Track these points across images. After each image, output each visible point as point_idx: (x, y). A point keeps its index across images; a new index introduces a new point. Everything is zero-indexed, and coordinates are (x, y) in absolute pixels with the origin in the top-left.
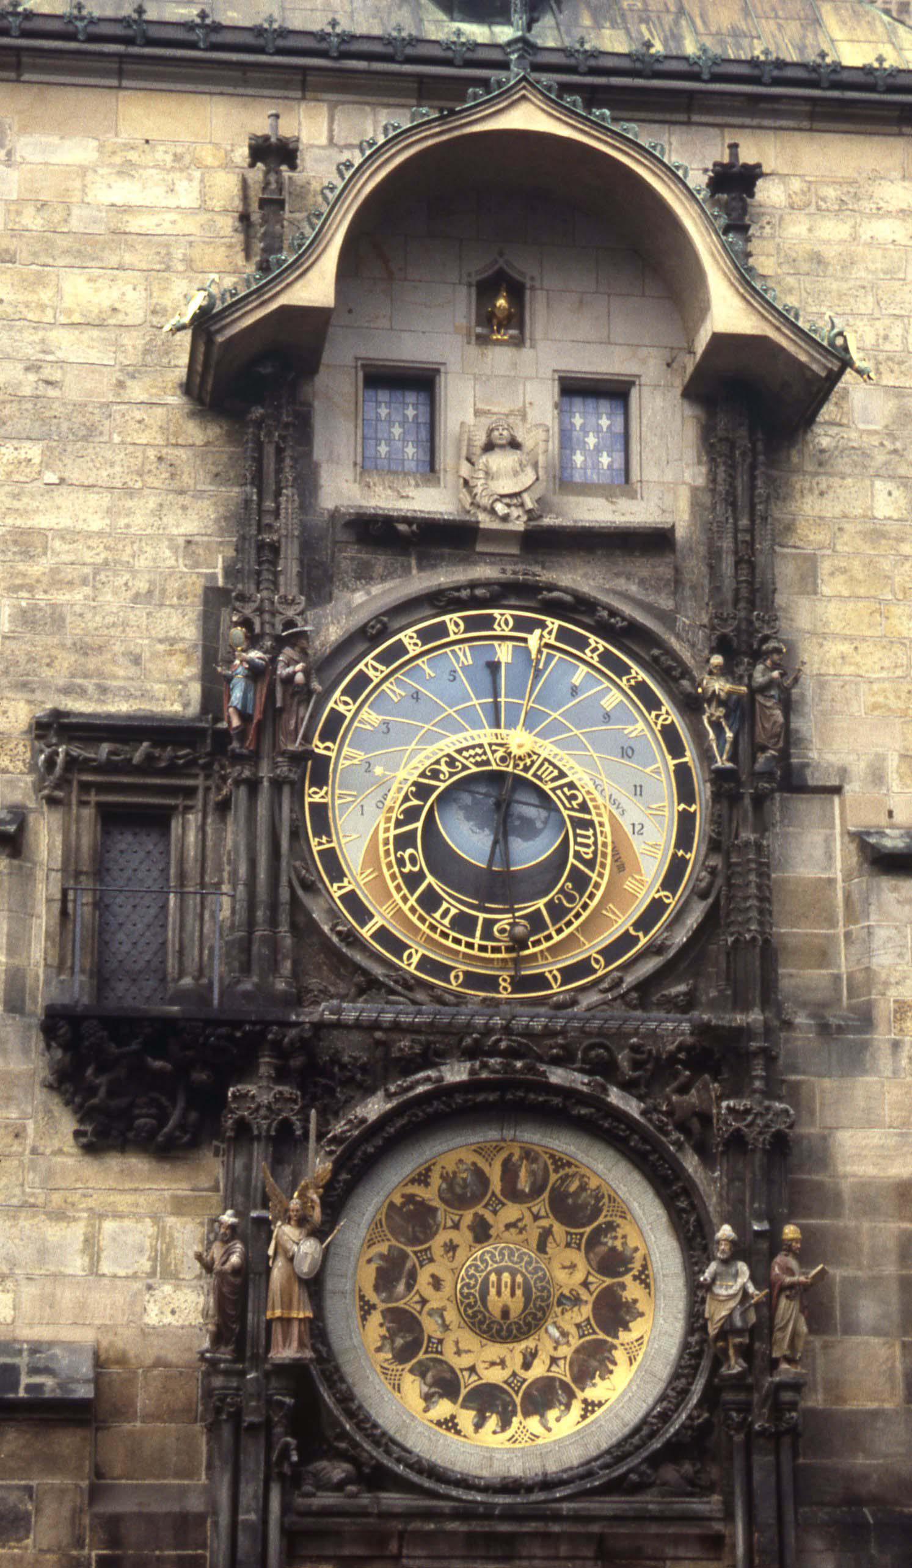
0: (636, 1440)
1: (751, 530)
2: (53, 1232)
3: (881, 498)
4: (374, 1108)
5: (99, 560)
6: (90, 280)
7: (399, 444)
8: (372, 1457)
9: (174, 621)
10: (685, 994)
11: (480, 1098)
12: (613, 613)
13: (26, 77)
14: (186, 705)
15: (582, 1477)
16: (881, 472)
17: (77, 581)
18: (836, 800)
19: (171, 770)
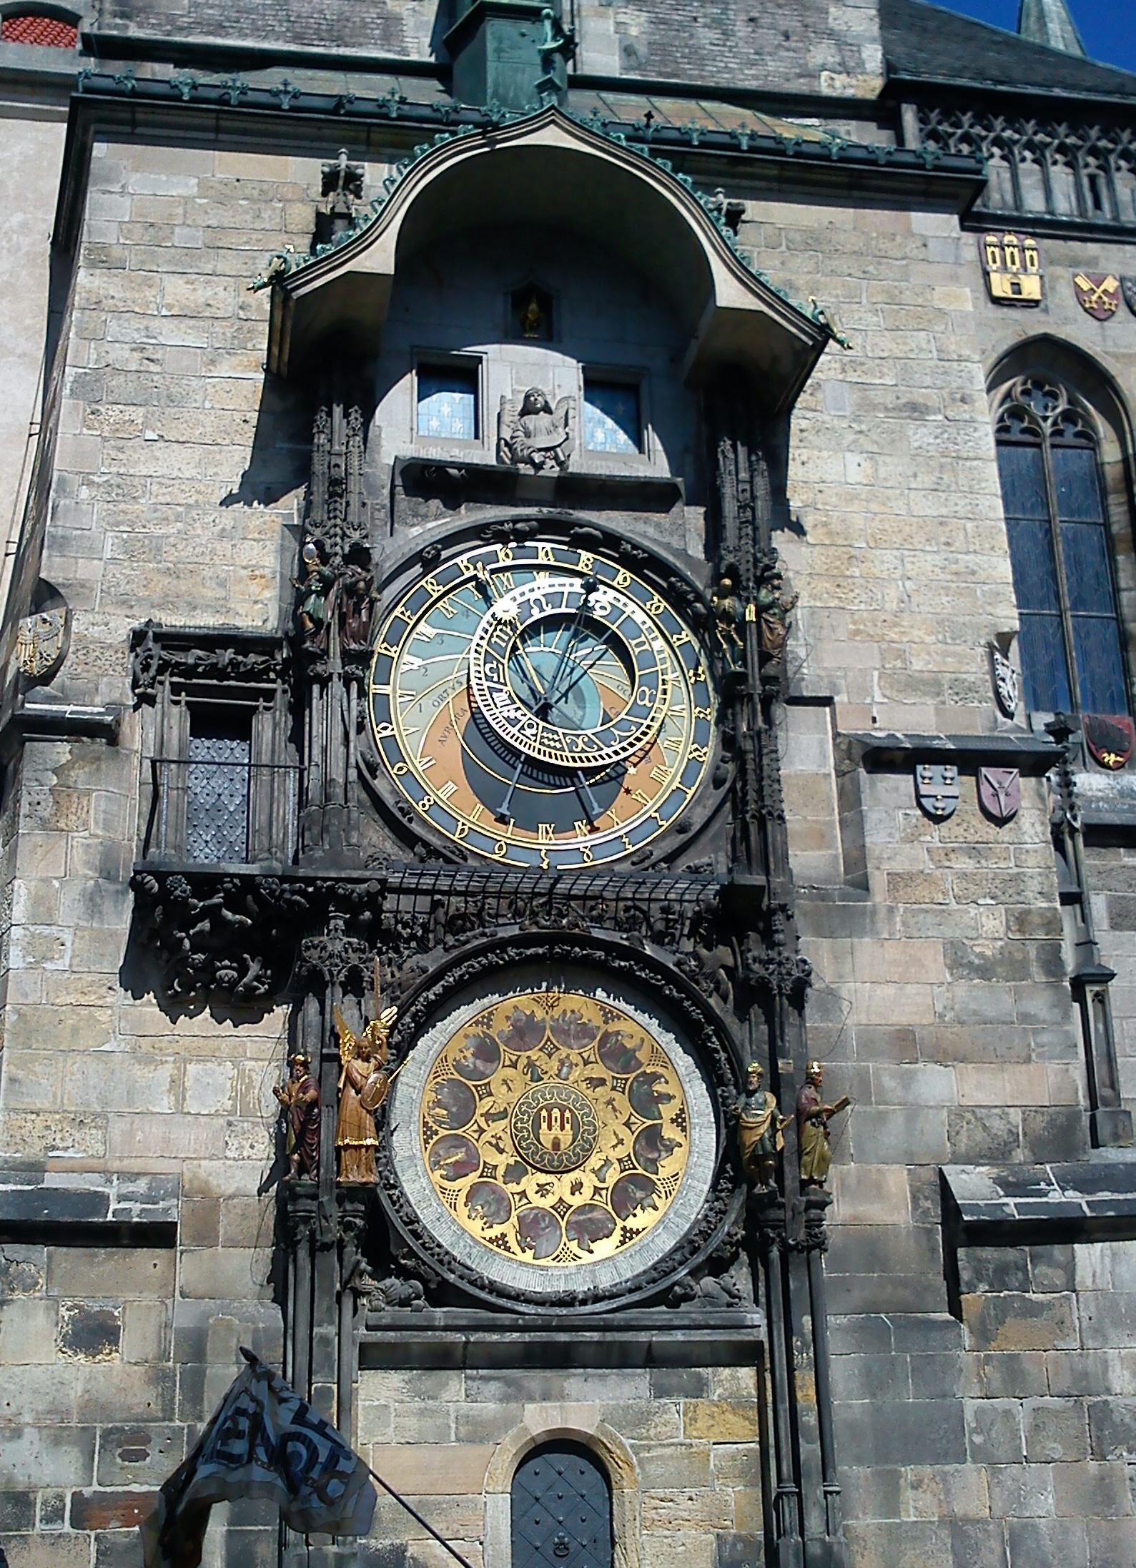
0: (678, 1257)
1: (751, 482)
2: (141, 1073)
3: (852, 468)
4: (432, 961)
5: (191, 501)
6: (187, 283)
7: (447, 420)
8: (438, 1274)
9: (255, 552)
10: (709, 865)
11: (529, 952)
12: (635, 547)
13: (139, 130)
14: (265, 621)
15: (631, 1291)
16: (852, 448)
17: (172, 518)
18: (827, 709)
19: (252, 675)
